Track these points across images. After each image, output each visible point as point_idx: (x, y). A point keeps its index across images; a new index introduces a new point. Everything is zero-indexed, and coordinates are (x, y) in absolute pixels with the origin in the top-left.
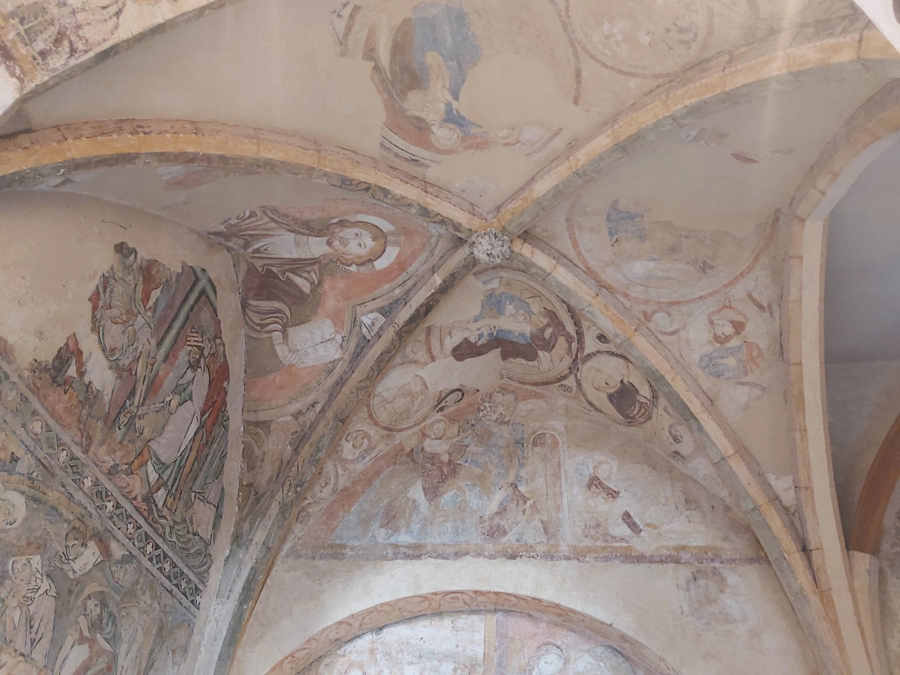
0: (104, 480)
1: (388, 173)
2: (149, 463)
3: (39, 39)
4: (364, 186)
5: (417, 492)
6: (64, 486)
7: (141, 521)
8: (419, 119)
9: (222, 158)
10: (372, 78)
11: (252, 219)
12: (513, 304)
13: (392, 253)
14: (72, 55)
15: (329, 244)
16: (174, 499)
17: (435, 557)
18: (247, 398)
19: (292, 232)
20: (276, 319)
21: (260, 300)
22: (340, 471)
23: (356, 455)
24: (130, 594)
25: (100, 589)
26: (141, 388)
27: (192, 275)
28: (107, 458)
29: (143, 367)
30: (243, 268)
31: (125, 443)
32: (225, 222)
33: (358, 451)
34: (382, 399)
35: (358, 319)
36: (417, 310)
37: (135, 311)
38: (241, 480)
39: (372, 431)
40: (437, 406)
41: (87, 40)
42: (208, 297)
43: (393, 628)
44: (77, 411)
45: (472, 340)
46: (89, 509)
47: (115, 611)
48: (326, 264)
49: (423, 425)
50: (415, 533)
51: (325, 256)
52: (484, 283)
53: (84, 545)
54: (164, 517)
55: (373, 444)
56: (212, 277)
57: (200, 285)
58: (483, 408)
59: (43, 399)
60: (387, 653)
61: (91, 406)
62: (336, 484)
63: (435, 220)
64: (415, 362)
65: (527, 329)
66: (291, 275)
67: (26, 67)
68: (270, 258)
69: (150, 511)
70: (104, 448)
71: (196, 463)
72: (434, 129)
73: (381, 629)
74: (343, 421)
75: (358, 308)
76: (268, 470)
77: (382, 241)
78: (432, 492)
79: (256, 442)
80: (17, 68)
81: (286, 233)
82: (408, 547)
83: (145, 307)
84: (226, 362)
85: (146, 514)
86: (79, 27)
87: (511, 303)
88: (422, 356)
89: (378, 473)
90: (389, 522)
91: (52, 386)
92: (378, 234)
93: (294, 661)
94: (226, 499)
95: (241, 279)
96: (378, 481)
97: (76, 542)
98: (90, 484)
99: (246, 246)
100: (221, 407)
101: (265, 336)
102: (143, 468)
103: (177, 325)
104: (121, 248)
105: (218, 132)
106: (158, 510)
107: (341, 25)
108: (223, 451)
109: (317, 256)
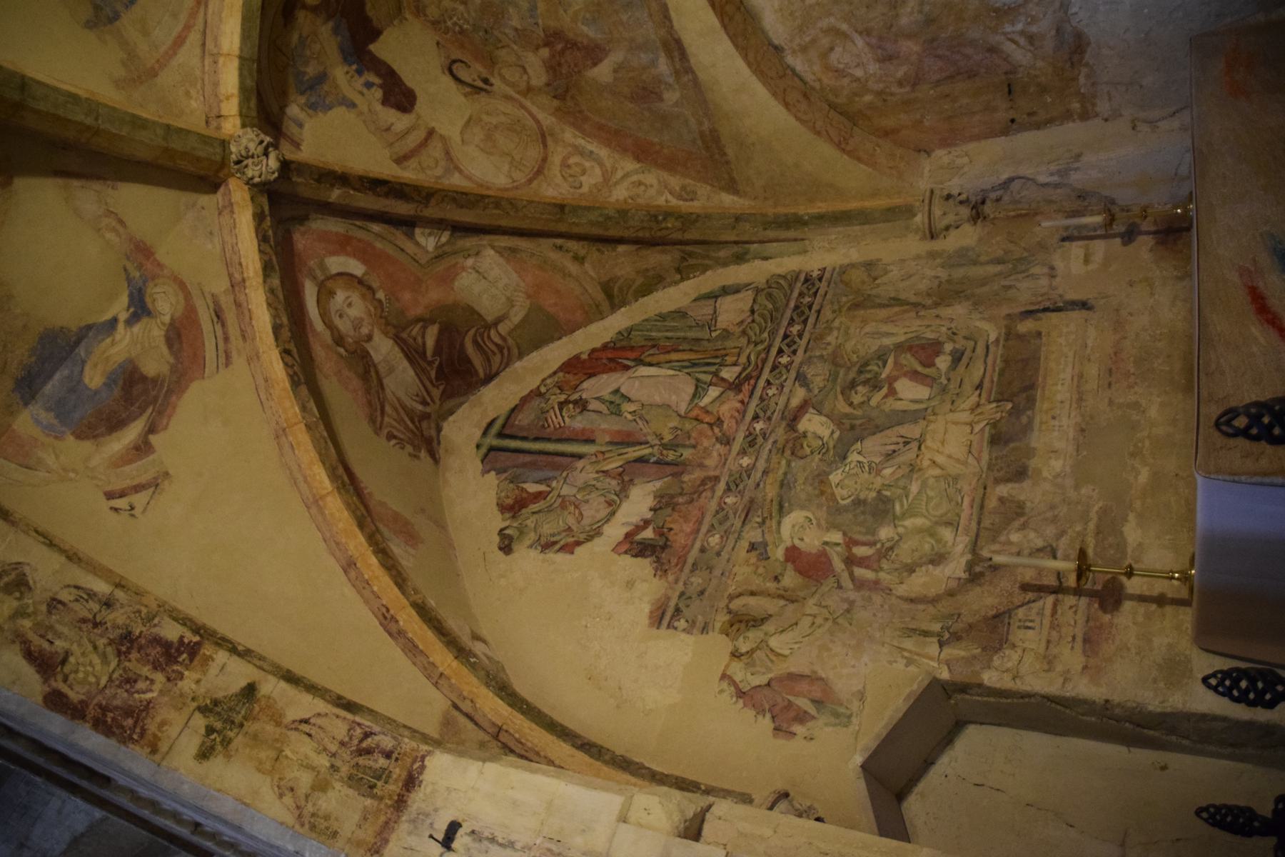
0: (736, 447)
1: (254, 339)
2: (702, 404)
3: (378, 766)
4: (288, 359)
5: (603, 72)
6: (758, 485)
7: (762, 383)
8: (169, 342)
9: (361, 526)
10: (166, 428)
11: (396, 433)
12: (302, 69)
13: (336, 264)
14: (371, 733)
15: (369, 338)
16: (726, 355)
17: (670, 20)
18: (588, 321)
19: (383, 389)
20: (486, 339)
21: (474, 368)
22: (619, 174)
23: (593, 164)
24: (835, 360)
25: (840, 397)
26: (634, 453)
27: (491, 457)
28: (715, 454)
29: (610, 463)
30: (450, 403)
31: (692, 441)
32: (415, 456)
33: (587, 164)
34: (513, 169)
35: (436, 254)
36: (387, 195)
37: (560, 500)
38: (676, 283)
39: (556, 159)
40: (485, 90)
41: (349, 730)
42: (504, 426)
43: (771, 34)
44: (683, 508)
45: (378, 94)
46: (770, 446)
47: (855, 369)
48: (395, 327)
49: (517, 96)
50: (651, 56)
51: (386, 334)
52: (301, 126)
53: (805, 435)
54: (749, 357)
55: (570, 149)
56: (479, 433)
57: (496, 442)
58: (457, 28)
59: (687, 548)
60: (800, 31)
61: (672, 497)
62: (636, 172)
63: (268, 250)
64: (447, 153)
65: (325, 30)
66: (429, 353)
67: (409, 760)
68: (424, 386)
69: (748, 378)
70: (707, 462)
71: (681, 348)
72: (167, 319)
73: (776, 48)
74: (562, 207)
75: (423, 262)
76: (657, 259)
77: (330, 284)
78: (594, 53)
79: (630, 286)
80: (415, 767)
81: (388, 391)
82: (673, 61)
83: (550, 492)
84: (561, 369)
85: (752, 382)
86: (342, 744)
87: (305, 73)
88: (435, 150)
89: (601, 127)
90: (652, 92)
91: (671, 547)
92: (325, 294)
93: (845, 139)
94: (704, 290)
95: (462, 399)
96: (610, 124)
97: (805, 445)
98: (746, 458)
99: (426, 416)
100: (610, 348)
101: (510, 341)
102: (709, 409)
103: (550, 447)
104: (506, 548)
105: (337, 544)
106: (744, 369)
107: (139, 499)
108: (656, 320)
109: (391, 342)
